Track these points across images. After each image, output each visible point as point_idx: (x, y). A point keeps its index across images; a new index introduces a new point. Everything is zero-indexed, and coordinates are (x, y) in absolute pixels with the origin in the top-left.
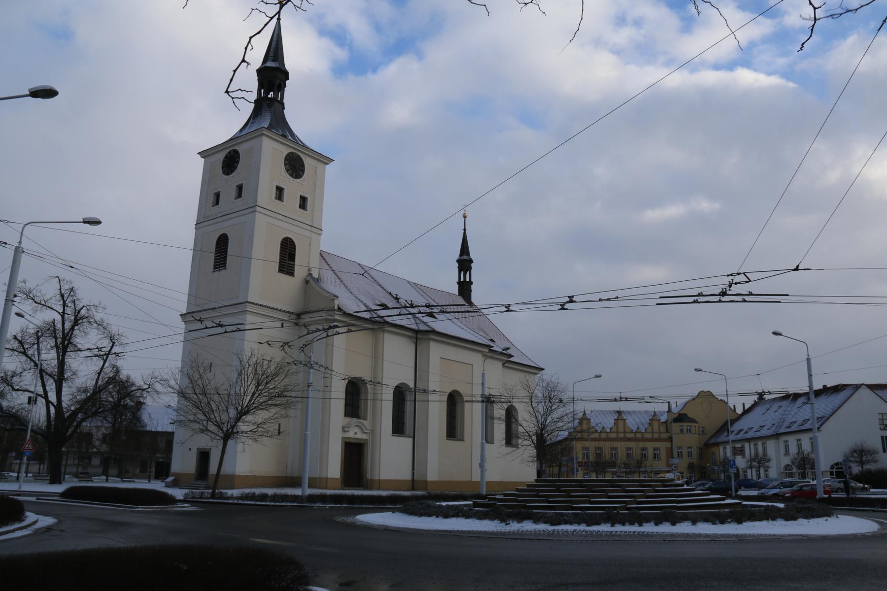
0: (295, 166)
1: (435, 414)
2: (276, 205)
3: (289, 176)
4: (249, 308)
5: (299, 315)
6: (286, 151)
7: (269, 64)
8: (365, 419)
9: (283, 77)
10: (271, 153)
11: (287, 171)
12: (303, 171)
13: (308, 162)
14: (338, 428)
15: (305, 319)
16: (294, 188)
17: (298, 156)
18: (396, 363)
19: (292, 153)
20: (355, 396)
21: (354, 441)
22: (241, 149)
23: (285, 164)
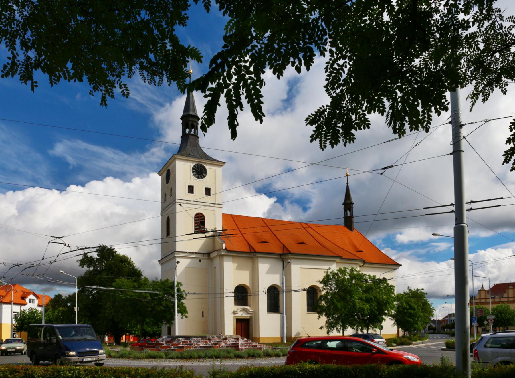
0: (200, 172)
1: (299, 301)
2: (190, 197)
3: (196, 178)
4: (177, 254)
5: (209, 254)
6: (192, 165)
7: (185, 114)
8: (250, 306)
9: (194, 119)
10: (183, 169)
11: (195, 175)
12: (206, 173)
13: (208, 167)
14: (231, 311)
15: (213, 255)
16: (200, 185)
17: (201, 165)
18: (267, 274)
19: (197, 165)
20: (242, 295)
21: (242, 318)
22: (170, 168)
23: (193, 172)
